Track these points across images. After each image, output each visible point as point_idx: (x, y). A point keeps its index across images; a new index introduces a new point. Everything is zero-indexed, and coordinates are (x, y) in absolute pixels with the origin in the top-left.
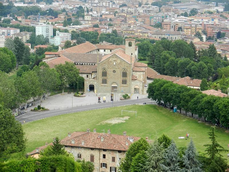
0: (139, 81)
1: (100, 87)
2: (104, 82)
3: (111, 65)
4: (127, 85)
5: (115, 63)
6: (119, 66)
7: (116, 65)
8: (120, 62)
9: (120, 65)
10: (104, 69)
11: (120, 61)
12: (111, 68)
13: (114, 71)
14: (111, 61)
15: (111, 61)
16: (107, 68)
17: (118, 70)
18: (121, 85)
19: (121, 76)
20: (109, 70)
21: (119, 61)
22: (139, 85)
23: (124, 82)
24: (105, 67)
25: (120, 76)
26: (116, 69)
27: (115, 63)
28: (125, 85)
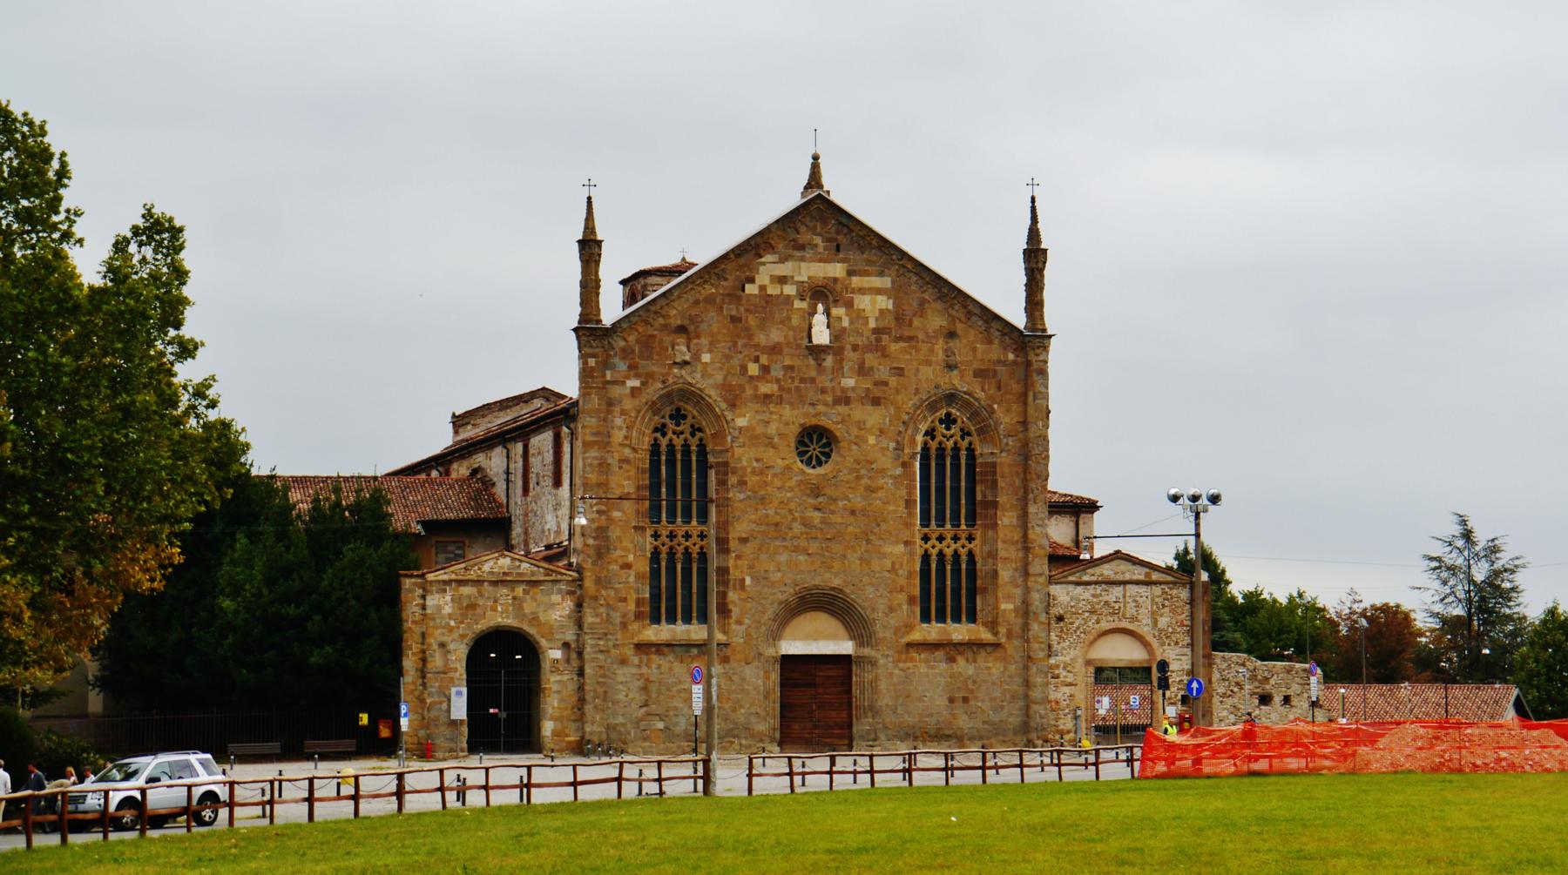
0: (1139, 573)
1: (624, 662)
2: (682, 587)
3: (775, 350)
4: (993, 626)
5: (819, 320)
6: (883, 372)
7: (836, 347)
8: (899, 317)
9: (894, 347)
10: (678, 416)
11: (895, 292)
12: (767, 396)
13: (816, 442)
14: (766, 299)
15: (773, 290)
16: (713, 395)
17: (874, 417)
18: (916, 636)
19: (909, 503)
20: (741, 422)
21: (884, 303)
22: (1145, 629)
23: (951, 589)
24: (695, 378)
25: (902, 509)
26: (841, 409)
27: (819, 320)
28: (960, 632)
